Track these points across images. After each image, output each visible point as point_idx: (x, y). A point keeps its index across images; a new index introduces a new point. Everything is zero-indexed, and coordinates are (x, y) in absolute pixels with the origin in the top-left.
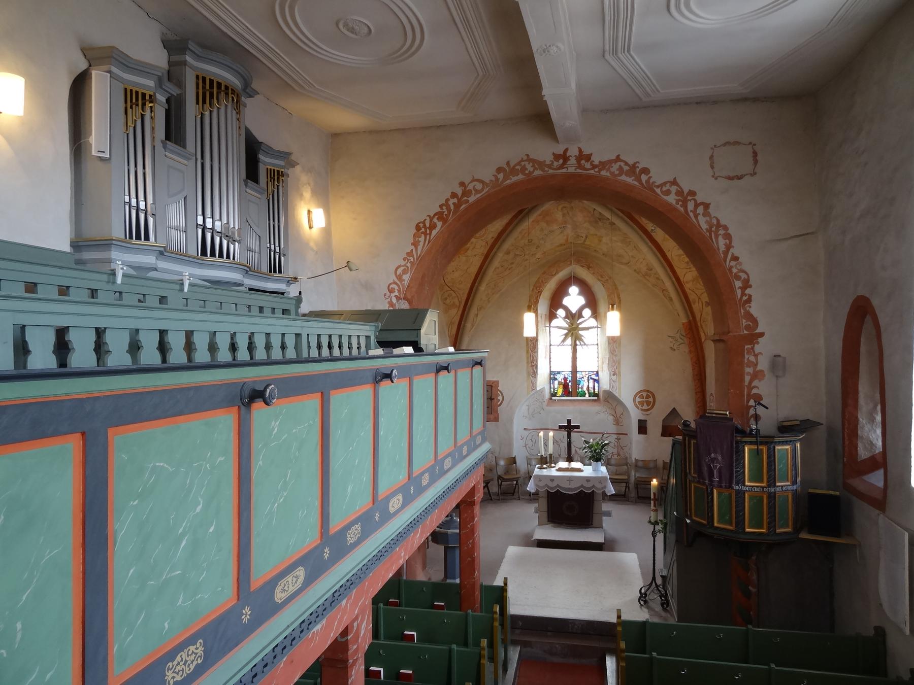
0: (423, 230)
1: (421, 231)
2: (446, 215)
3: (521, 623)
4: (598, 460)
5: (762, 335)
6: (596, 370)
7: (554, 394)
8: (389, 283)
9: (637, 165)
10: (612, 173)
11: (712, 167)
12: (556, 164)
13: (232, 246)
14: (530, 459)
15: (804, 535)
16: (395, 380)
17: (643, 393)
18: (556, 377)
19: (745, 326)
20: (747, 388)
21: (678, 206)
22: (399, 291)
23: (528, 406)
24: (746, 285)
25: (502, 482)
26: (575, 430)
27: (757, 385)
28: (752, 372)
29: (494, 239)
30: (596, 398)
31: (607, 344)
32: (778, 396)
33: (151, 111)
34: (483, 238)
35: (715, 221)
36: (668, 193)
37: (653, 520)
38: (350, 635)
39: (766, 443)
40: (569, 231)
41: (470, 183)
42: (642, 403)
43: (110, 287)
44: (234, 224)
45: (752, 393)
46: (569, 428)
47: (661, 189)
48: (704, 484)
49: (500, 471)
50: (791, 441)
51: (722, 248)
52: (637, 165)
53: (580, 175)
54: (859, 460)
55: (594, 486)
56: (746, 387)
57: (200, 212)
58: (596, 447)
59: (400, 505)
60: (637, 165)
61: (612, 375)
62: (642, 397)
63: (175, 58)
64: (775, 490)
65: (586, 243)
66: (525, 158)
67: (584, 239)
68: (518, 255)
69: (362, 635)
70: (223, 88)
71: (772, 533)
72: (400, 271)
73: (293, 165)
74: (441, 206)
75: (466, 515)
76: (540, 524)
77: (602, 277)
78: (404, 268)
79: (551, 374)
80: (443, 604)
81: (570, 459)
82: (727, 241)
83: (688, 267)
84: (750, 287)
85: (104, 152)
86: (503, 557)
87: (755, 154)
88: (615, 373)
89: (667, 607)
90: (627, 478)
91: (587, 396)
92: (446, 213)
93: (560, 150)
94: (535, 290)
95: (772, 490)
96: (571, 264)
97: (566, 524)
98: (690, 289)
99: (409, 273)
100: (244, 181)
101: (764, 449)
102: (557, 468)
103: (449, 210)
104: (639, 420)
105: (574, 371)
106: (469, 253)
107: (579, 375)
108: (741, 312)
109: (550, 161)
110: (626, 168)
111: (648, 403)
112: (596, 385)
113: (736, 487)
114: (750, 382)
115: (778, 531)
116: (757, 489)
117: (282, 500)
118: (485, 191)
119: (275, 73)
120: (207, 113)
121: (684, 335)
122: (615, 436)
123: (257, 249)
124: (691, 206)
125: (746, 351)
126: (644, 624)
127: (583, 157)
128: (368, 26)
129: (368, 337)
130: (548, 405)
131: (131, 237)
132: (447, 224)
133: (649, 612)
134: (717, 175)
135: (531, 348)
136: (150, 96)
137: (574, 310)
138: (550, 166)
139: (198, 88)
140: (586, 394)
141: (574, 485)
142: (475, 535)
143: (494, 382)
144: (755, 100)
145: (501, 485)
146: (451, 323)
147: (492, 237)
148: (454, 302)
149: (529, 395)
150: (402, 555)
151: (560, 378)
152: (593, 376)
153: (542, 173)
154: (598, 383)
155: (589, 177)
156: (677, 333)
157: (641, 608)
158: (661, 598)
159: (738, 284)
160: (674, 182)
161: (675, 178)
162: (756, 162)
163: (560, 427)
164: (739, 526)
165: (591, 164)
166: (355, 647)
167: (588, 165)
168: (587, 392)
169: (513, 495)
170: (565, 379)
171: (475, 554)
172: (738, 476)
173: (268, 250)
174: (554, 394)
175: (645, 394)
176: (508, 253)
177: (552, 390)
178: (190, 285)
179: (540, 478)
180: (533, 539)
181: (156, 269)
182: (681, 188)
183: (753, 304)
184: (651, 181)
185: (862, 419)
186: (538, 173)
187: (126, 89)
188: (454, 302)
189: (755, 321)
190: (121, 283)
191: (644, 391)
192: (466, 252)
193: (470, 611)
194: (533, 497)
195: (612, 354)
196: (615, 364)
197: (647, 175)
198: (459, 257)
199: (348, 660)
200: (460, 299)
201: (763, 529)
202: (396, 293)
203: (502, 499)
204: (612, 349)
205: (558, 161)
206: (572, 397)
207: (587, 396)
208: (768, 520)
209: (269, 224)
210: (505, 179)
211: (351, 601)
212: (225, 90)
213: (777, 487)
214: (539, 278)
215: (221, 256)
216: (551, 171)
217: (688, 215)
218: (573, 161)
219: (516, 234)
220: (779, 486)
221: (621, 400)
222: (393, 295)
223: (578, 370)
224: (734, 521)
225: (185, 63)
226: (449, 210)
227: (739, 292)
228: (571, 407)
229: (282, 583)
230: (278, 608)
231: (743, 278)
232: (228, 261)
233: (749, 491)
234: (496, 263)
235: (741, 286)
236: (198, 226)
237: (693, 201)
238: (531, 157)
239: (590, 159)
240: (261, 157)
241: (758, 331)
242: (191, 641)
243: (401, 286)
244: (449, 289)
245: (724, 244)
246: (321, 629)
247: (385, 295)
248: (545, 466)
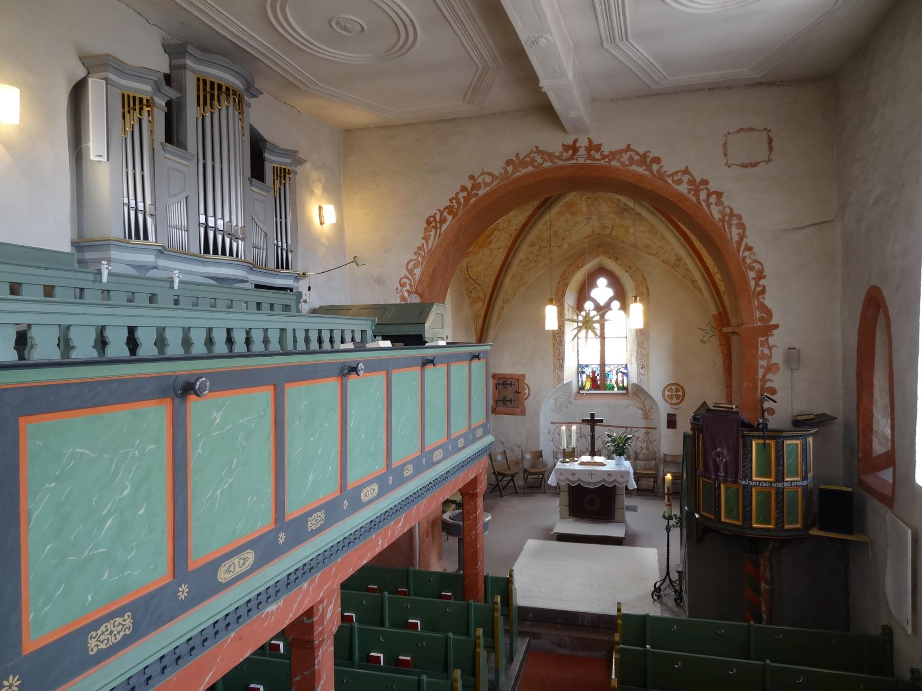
0: (433, 224)
1: (432, 225)
2: (456, 208)
3: (531, 615)
4: (620, 454)
5: (776, 327)
6: (625, 363)
7: (582, 388)
8: (400, 278)
9: (648, 154)
10: (622, 163)
11: (725, 155)
12: (565, 155)
13: (235, 244)
14: (556, 452)
15: (814, 532)
16: (361, 373)
17: (672, 387)
18: (584, 370)
19: (759, 317)
20: (761, 381)
21: (690, 196)
22: (410, 285)
23: (555, 399)
24: (760, 275)
25: (527, 476)
26: (598, 424)
27: (771, 378)
28: (766, 365)
29: (517, 231)
30: (625, 391)
31: (635, 336)
32: (792, 389)
33: (149, 115)
35: (728, 211)
36: (679, 182)
37: (667, 515)
38: (316, 617)
39: (774, 438)
40: (595, 222)
41: (479, 176)
42: (671, 397)
43: (97, 286)
44: (238, 221)
45: (766, 387)
46: (592, 422)
47: (673, 178)
48: (710, 478)
49: (527, 465)
50: (801, 436)
51: (735, 238)
52: (648, 154)
53: (589, 166)
55: (615, 480)
56: (759, 380)
57: (202, 211)
58: (619, 441)
59: (375, 494)
60: (647, 155)
61: (640, 368)
62: (671, 390)
63: (176, 62)
64: (783, 485)
65: (613, 234)
66: (534, 149)
67: (609, 230)
68: (543, 247)
69: (328, 618)
70: (224, 89)
71: (780, 529)
72: (411, 265)
73: (301, 162)
74: (451, 200)
75: (469, 507)
76: (562, 518)
77: (630, 269)
78: (414, 262)
79: (578, 368)
80: (450, 594)
81: (593, 454)
82: (741, 231)
84: (765, 277)
85: (102, 156)
86: (522, 550)
87: (770, 141)
88: (643, 366)
89: (681, 602)
90: (654, 472)
91: (616, 389)
92: (456, 206)
93: (569, 141)
94: (562, 283)
95: (780, 485)
96: (598, 255)
97: (587, 518)
99: (420, 268)
100: (249, 179)
101: (772, 443)
102: (579, 462)
103: (459, 204)
104: (668, 414)
105: (603, 365)
106: (493, 246)
107: (607, 369)
108: (754, 303)
109: (560, 152)
110: (637, 158)
111: (677, 397)
112: (625, 378)
113: (743, 482)
114: (764, 376)
115: (786, 527)
116: (764, 484)
117: (226, 486)
118: (495, 183)
119: (279, 74)
120: (208, 115)
121: (715, 326)
122: (644, 430)
123: (263, 246)
124: (703, 195)
125: (760, 344)
126: (644, 619)
127: (593, 147)
128: (360, 24)
129: (363, 332)
130: (575, 399)
131: (130, 237)
132: (457, 218)
133: (661, 607)
134: (730, 162)
136: (148, 101)
137: (602, 303)
138: (559, 158)
139: (198, 90)
140: (614, 387)
141: (595, 479)
142: (478, 527)
143: (520, 375)
144: (771, 84)
145: (527, 479)
146: (477, 316)
147: (516, 230)
148: (479, 295)
149: (556, 389)
150: (380, 542)
151: (588, 371)
152: (623, 370)
153: (551, 164)
154: (627, 376)
155: (599, 168)
156: (708, 325)
157: (654, 603)
158: (675, 594)
159: (752, 275)
160: (686, 171)
161: (687, 167)
162: (771, 148)
163: (584, 421)
164: (747, 522)
165: (602, 155)
166: (321, 629)
167: (598, 156)
168: (615, 386)
169: (540, 489)
170: (594, 372)
171: (478, 545)
172: (745, 471)
173: (275, 247)
174: (582, 388)
175: (674, 387)
176: (533, 245)
177: (580, 383)
178: (180, 282)
179: (561, 472)
180: (554, 532)
181: (155, 268)
182: (693, 177)
183: (767, 295)
184: (662, 171)
185: (878, 413)
186: (547, 164)
187: (123, 95)
189: (769, 313)
190: (107, 282)
191: (673, 384)
192: (489, 245)
193: (471, 601)
194: (556, 491)
195: (641, 347)
196: (644, 357)
197: (658, 164)
198: (483, 250)
199: (313, 642)
200: (485, 293)
201: (770, 524)
202: (408, 288)
203: (527, 493)
204: (640, 342)
205: (568, 152)
206: (600, 390)
207: (616, 389)
209: (276, 222)
210: (515, 170)
211: (314, 585)
212: (225, 91)
213: (786, 482)
214: (565, 270)
215: (224, 253)
216: (560, 163)
217: (700, 203)
218: (582, 152)
219: (540, 225)
220: (788, 481)
221: (650, 394)
222: (404, 289)
223: (606, 364)
224: (741, 516)
225: (184, 67)
226: (459, 204)
227: (753, 283)
228: (598, 401)
229: (227, 564)
230: (221, 587)
231: (756, 269)
232: (231, 258)
233: (757, 486)
234: (521, 255)
235: (755, 276)
236: (201, 225)
237: (705, 191)
238: (540, 149)
239: (600, 149)
240: (267, 155)
241: (773, 322)
242: (119, 613)
243: (412, 281)
244: (474, 282)
245: (737, 234)
246: (277, 610)
247: (397, 289)
248: (567, 460)
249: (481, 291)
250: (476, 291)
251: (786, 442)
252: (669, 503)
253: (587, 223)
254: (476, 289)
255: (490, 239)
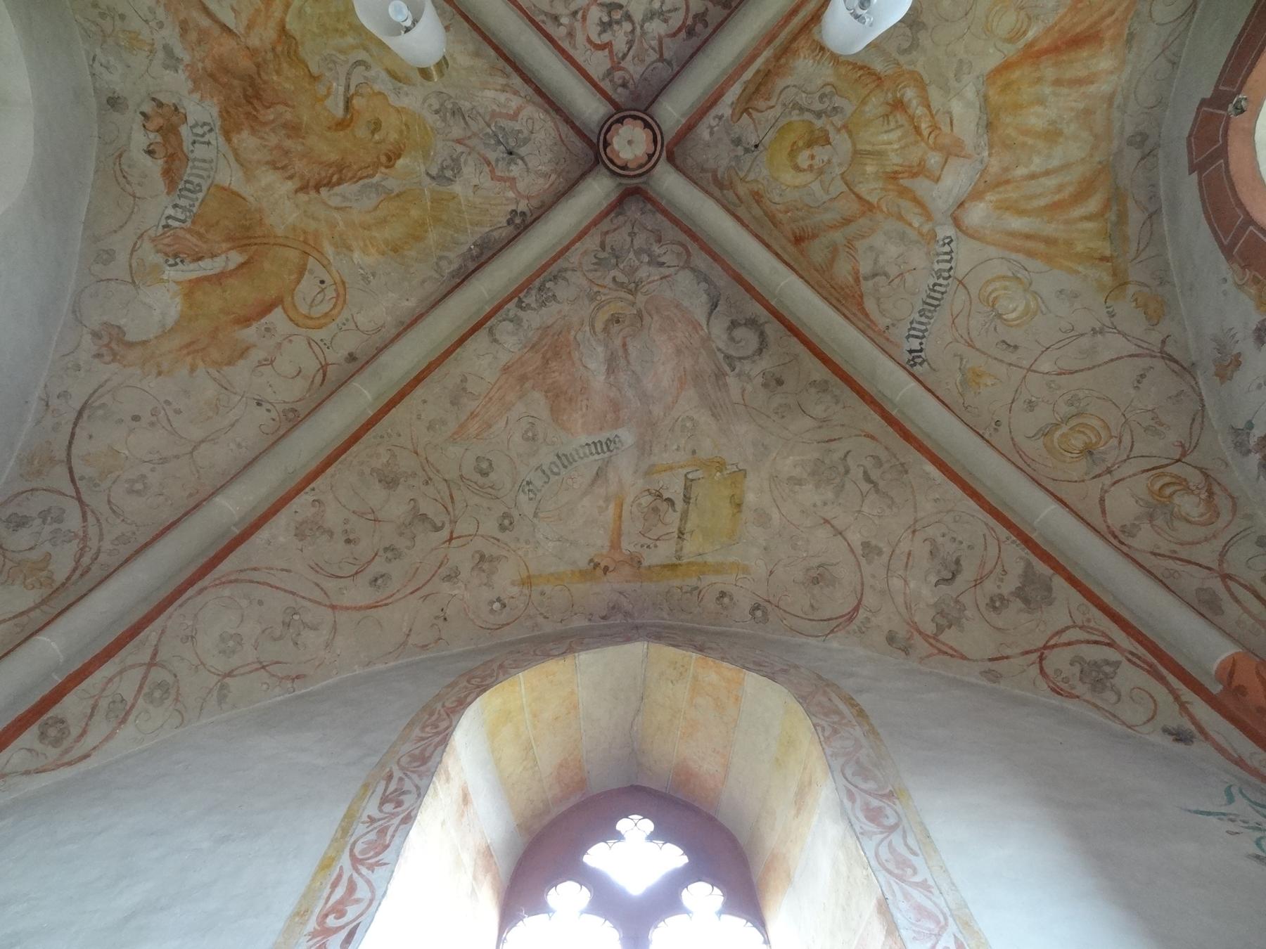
29: (353, 367)
34: (317, 335)
40: (625, 472)
67: (673, 518)
68: (424, 517)
83: (1097, 471)
98: (1155, 554)
106: (240, 373)
135: (359, 847)
147: (352, 358)
148: (48, 556)
188: (48, 556)
192: (230, 363)
198: (193, 369)
244: (74, 494)
249: (74, 546)
250: (48, 529)
253: (599, 475)
254: (59, 520)
255: (250, 333)
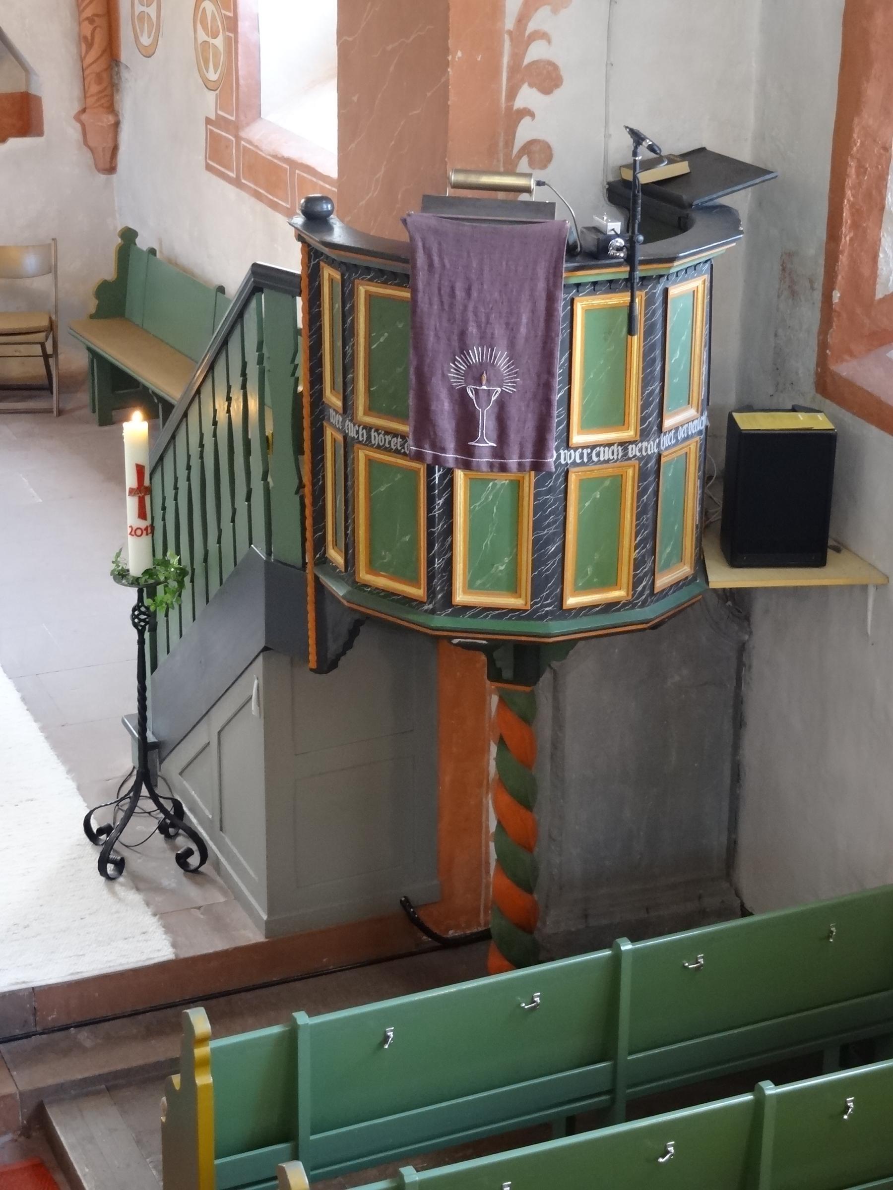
20: (511, 40)
27: (545, 27)
45: (527, 60)
54: (879, 295)
95: (650, 447)
114: (522, 19)
116: (605, 455)
208: (634, 555)
224: (526, 575)
251: (673, 291)
252: (143, 524)
